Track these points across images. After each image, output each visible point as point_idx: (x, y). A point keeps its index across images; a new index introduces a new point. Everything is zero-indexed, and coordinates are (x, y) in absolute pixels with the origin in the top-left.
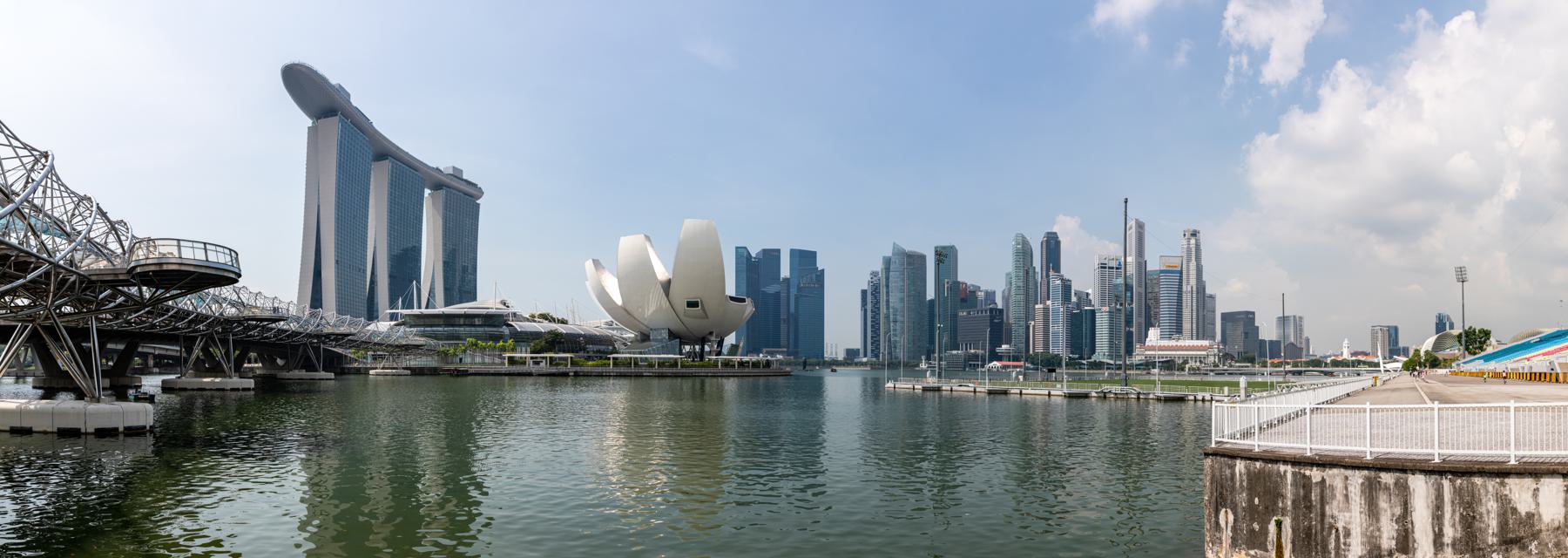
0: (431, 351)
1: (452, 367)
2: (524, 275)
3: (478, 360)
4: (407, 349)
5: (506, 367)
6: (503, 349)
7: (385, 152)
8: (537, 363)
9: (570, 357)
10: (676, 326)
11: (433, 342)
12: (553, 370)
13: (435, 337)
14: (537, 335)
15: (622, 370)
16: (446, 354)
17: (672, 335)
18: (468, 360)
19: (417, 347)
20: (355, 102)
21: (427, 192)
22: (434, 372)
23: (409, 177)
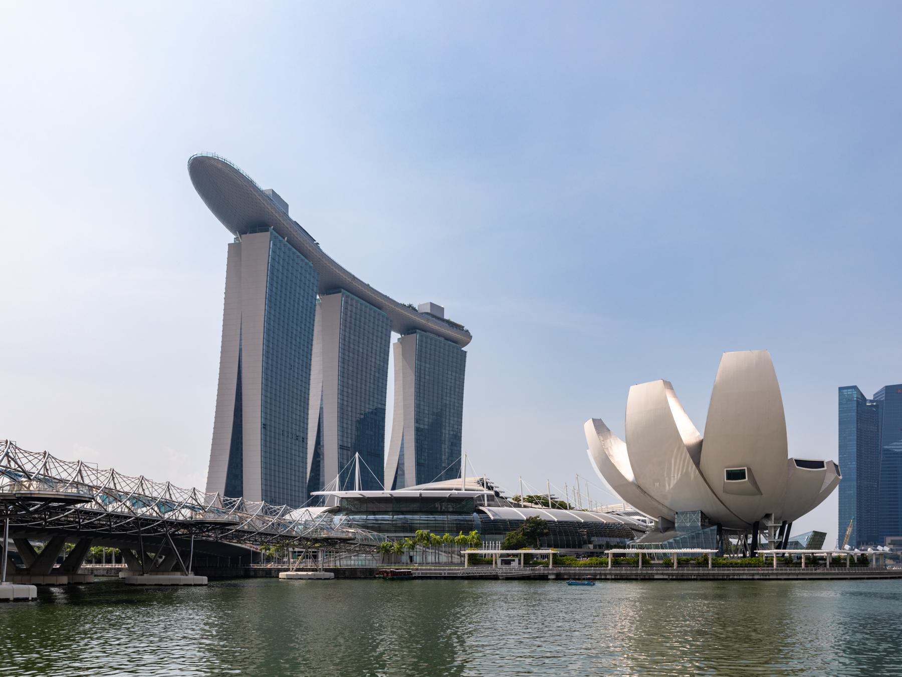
0: (365, 547)
1: (393, 568)
2: (532, 445)
3: (431, 558)
4: (331, 544)
5: (467, 568)
6: (464, 544)
7: (337, 283)
8: (508, 562)
9: (564, 548)
10: (713, 507)
11: (371, 535)
12: (528, 571)
13: (378, 528)
14: (515, 524)
15: (624, 571)
16: (387, 550)
17: (707, 519)
18: (418, 559)
19: (345, 541)
20: (293, 214)
21: (395, 337)
22: (368, 574)
23: (368, 314)
